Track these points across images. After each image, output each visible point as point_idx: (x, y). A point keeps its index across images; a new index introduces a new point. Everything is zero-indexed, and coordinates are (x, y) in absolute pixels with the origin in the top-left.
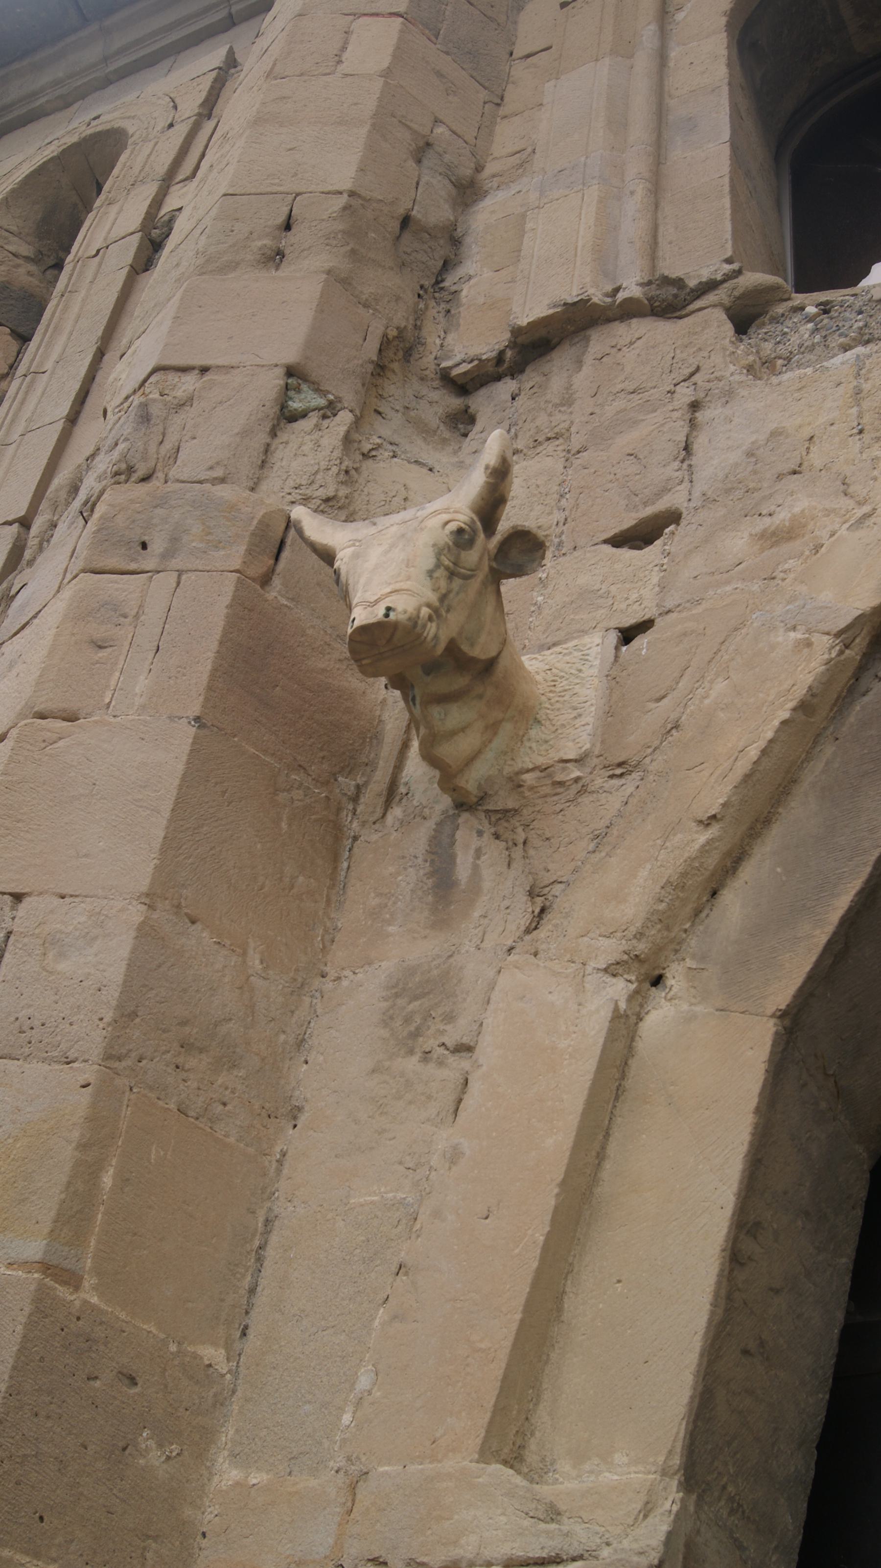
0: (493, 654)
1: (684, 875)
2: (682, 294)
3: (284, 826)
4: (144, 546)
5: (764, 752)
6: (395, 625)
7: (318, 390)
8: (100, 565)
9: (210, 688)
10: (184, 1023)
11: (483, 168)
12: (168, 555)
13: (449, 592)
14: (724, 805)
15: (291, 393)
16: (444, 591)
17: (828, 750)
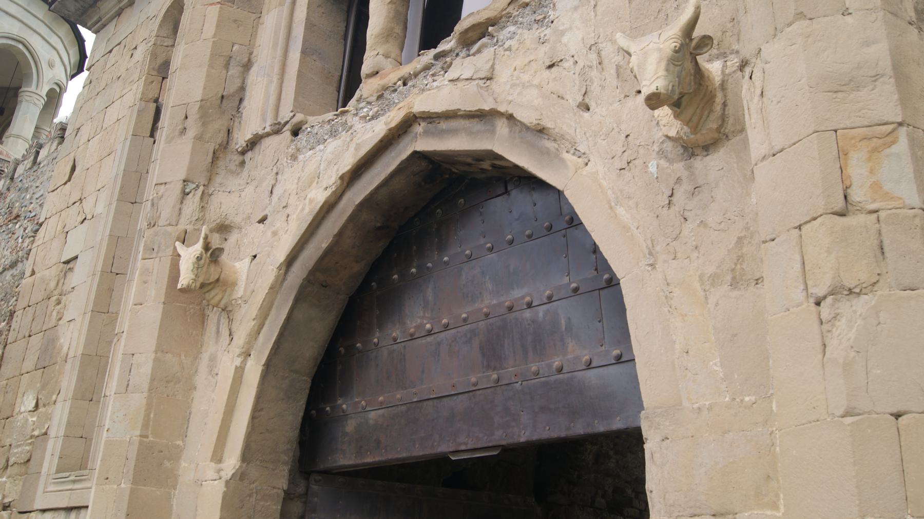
0: (216, 277)
1: (251, 332)
2: (280, 127)
3: (189, 320)
4: (153, 249)
5: (263, 301)
6: (184, 288)
7: (193, 183)
8: (144, 258)
9: (166, 293)
10: (166, 377)
11: (253, 52)
12: (158, 253)
13: (197, 273)
14: (256, 316)
15: (186, 187)
16: (196, 273)
17: (279, 296)
